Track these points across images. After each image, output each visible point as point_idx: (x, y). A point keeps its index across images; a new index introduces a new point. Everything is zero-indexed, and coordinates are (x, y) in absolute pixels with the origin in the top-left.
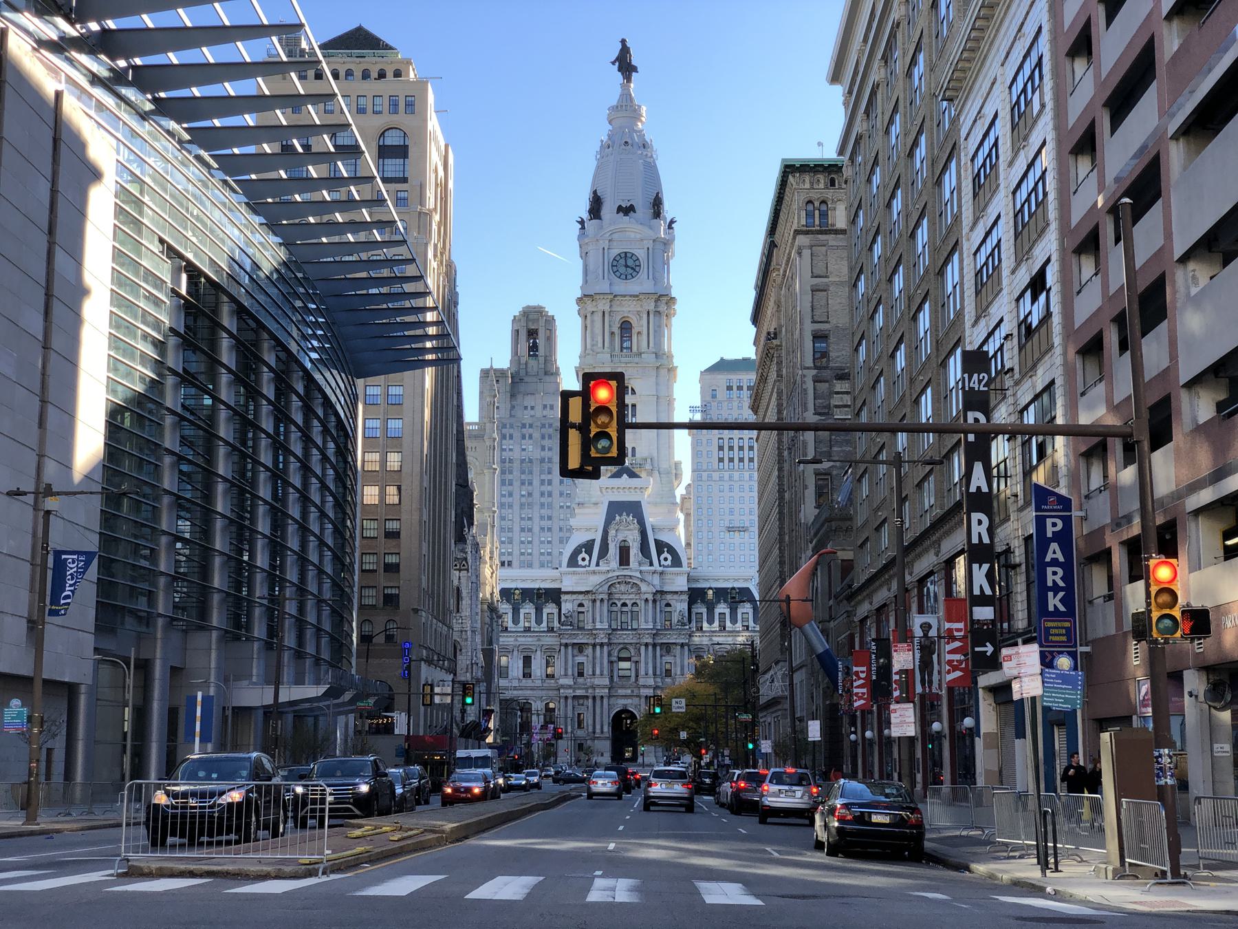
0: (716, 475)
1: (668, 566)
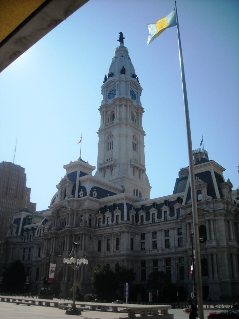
1: (82, 197)
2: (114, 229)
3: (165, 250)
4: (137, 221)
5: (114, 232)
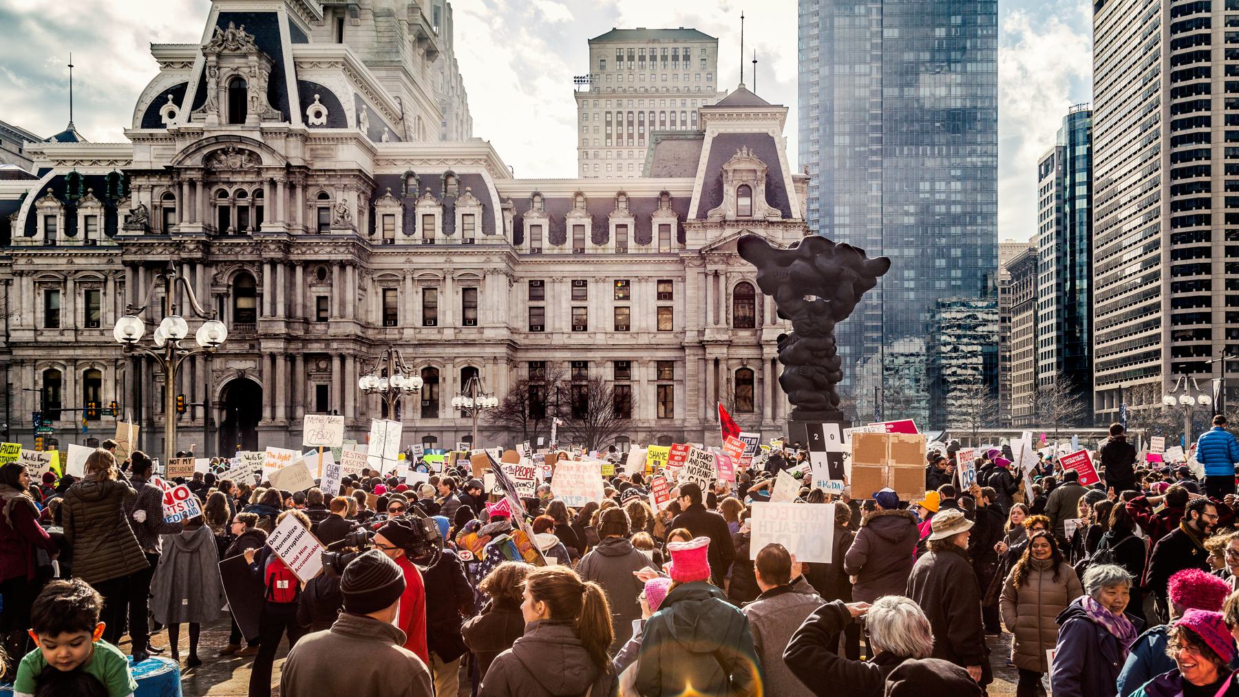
0: (602, 153)
1: (321, 126)
2: (456, 259)
3: (616, 336)
4: (518, 239)
5: (459, 266)
